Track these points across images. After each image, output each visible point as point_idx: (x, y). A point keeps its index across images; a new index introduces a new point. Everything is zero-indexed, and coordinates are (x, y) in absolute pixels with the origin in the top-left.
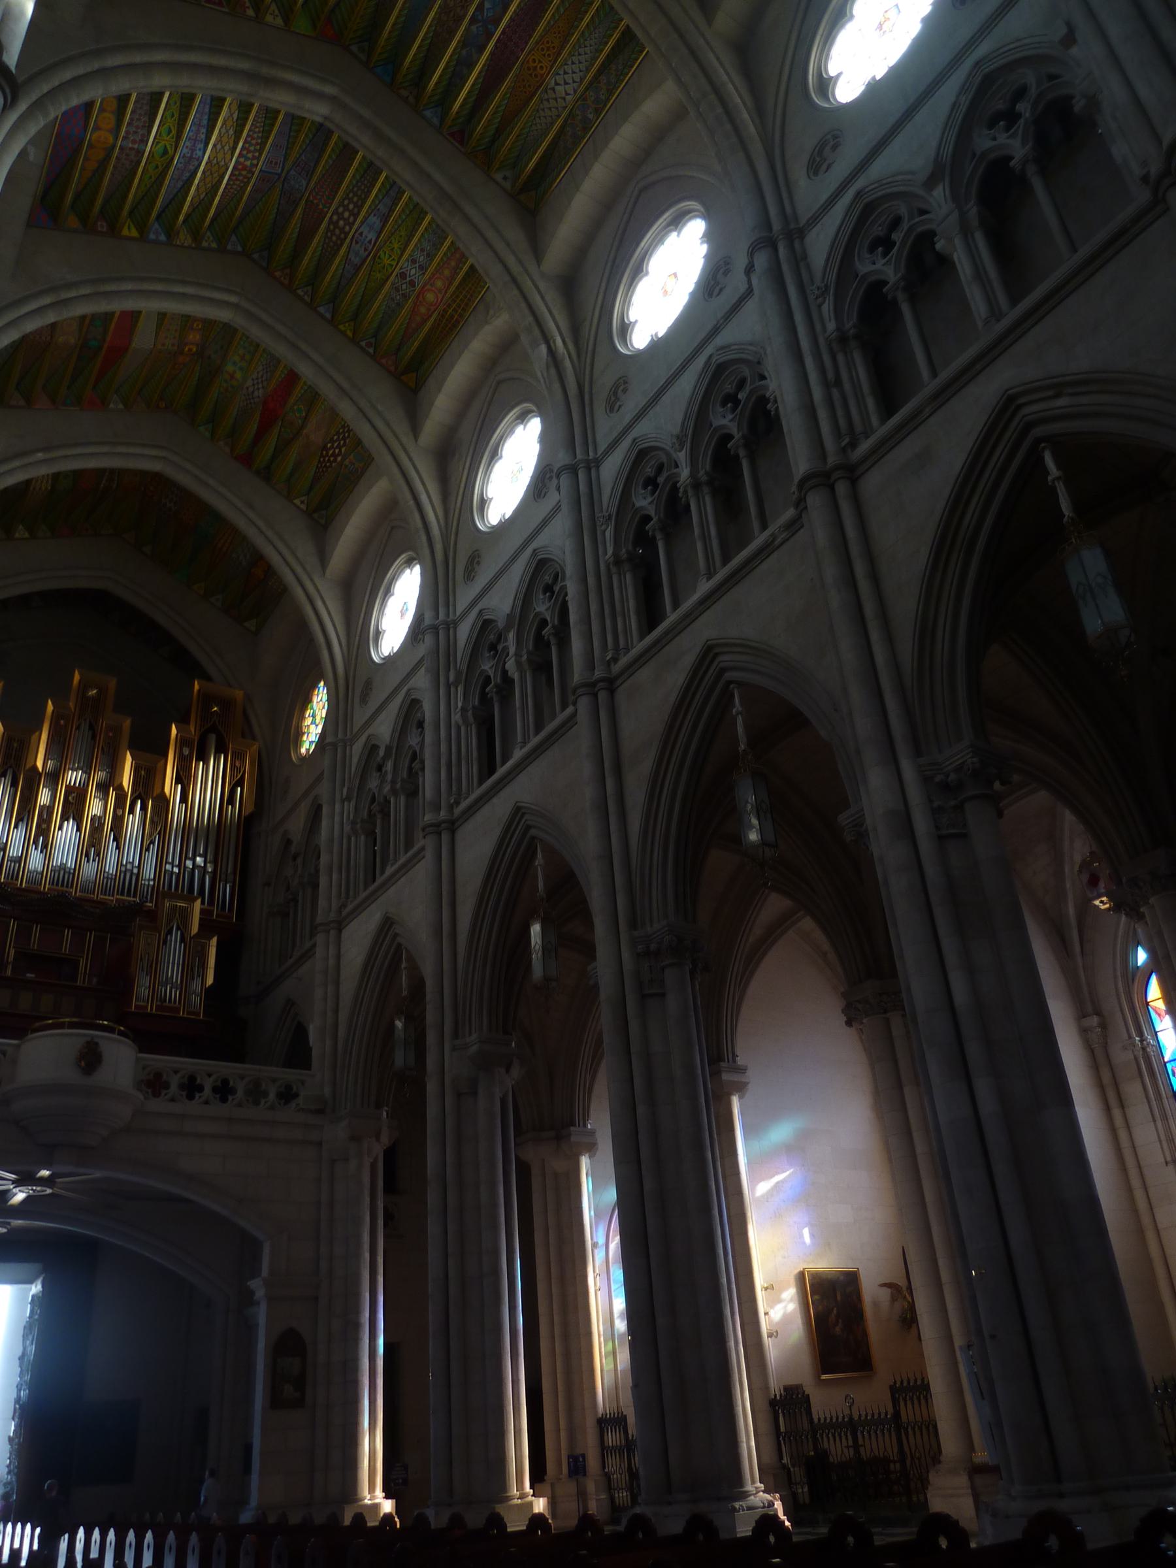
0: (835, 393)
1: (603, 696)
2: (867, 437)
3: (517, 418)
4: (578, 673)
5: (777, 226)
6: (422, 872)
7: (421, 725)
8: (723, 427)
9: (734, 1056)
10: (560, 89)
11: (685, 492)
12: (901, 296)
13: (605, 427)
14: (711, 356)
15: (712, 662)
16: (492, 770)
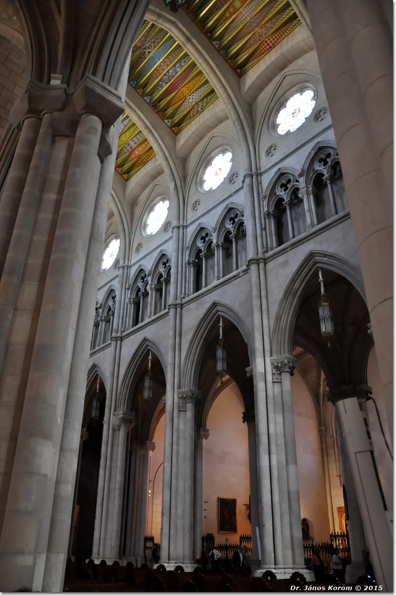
0: (264, 232)
1: (179, 309)
2: (272, 250)
3: (162, 199)
4: (171, 300)
5: (254, 171)
6: (110, 351)
7: (114, 298)
8: (229, 228)
9: (206, 426)
10: (191, 100)
11: (214, 248)
12: (288, 207)
13: (191, 215)
14: (228, 204)
15: (215, 307)
16: (137, 323)
